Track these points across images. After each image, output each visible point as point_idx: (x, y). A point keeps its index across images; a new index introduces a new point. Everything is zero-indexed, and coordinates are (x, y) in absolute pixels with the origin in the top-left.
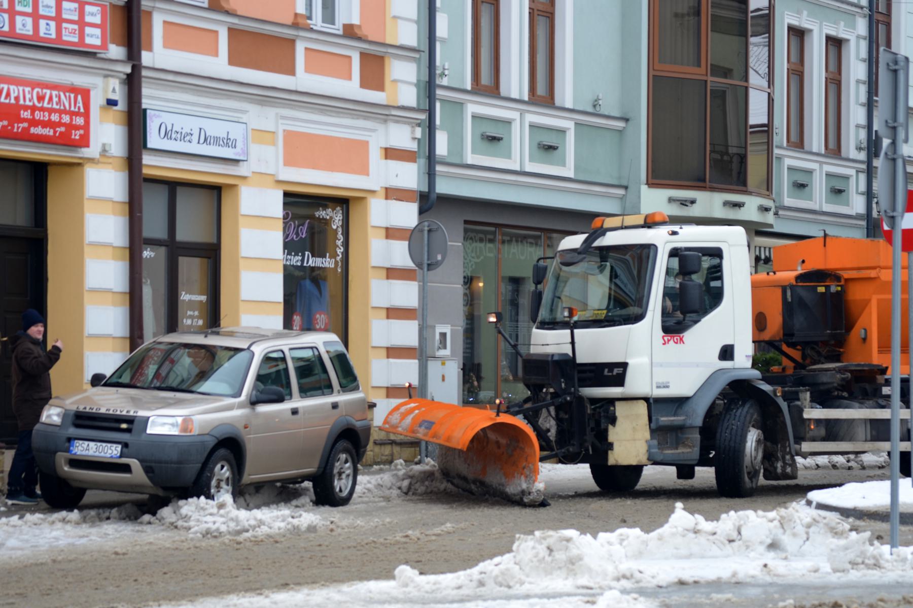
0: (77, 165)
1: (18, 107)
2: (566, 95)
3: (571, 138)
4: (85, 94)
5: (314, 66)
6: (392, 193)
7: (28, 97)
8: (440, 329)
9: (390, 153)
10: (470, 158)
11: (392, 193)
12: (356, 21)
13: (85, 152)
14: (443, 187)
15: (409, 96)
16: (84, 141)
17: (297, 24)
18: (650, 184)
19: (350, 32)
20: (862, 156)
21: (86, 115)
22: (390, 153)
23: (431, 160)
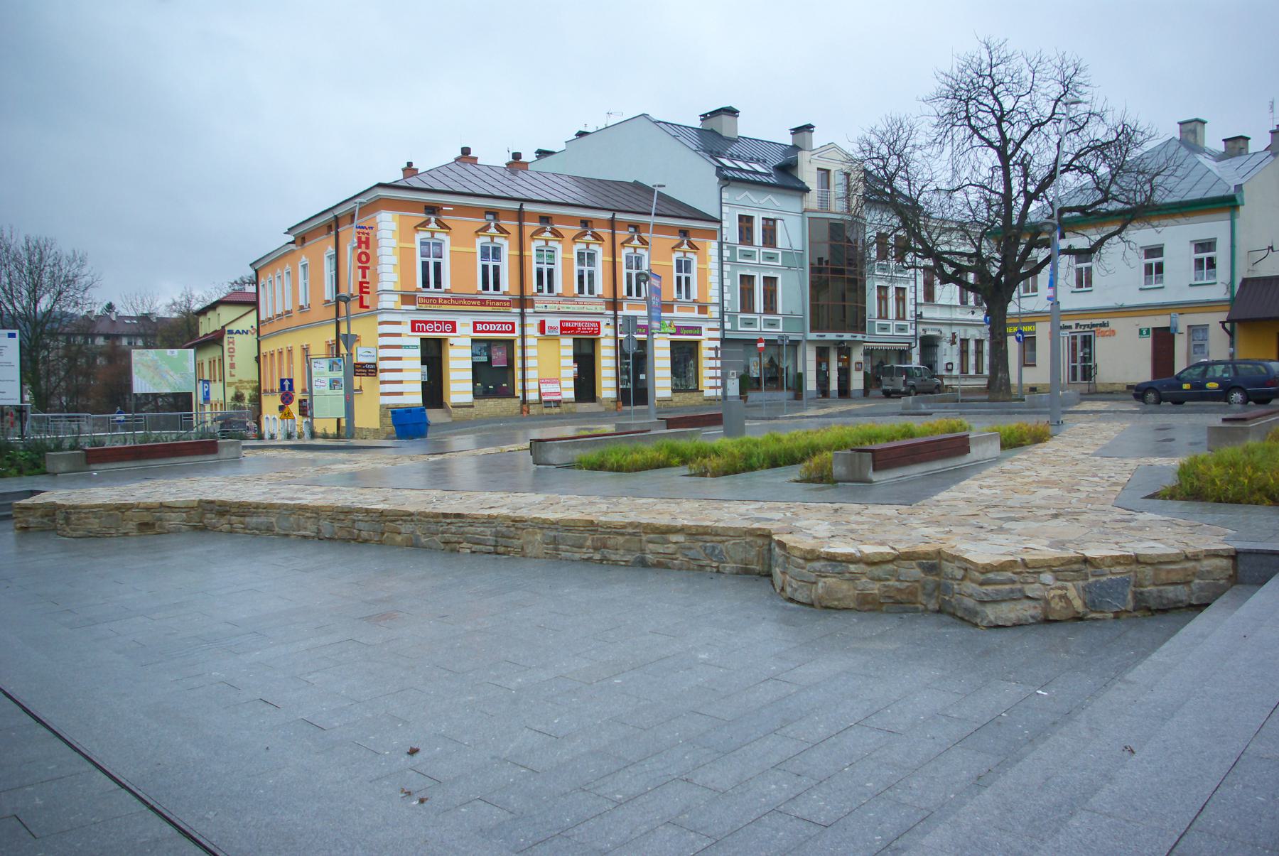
0: (599, 339)
1: (577, 327)
2: (780, 310)
3: (781, 322)
4: (599, 323)
5: (680, 309)
6: (710, 339)
7: (580, 325)
8: (731, 372)
9: (710, 329)
10: (740, 329)
11: (710, 339)
12: (696, 298)
13: (600, 336)
14: (727, 336)
15: (717, 315)
16: (599, 333)
17: (675, 301)
18: (811, 332)
19: (694, 301)
20: (914, 319)
21: (599, 327)
22: (710, 329)
23: (724, 330)
